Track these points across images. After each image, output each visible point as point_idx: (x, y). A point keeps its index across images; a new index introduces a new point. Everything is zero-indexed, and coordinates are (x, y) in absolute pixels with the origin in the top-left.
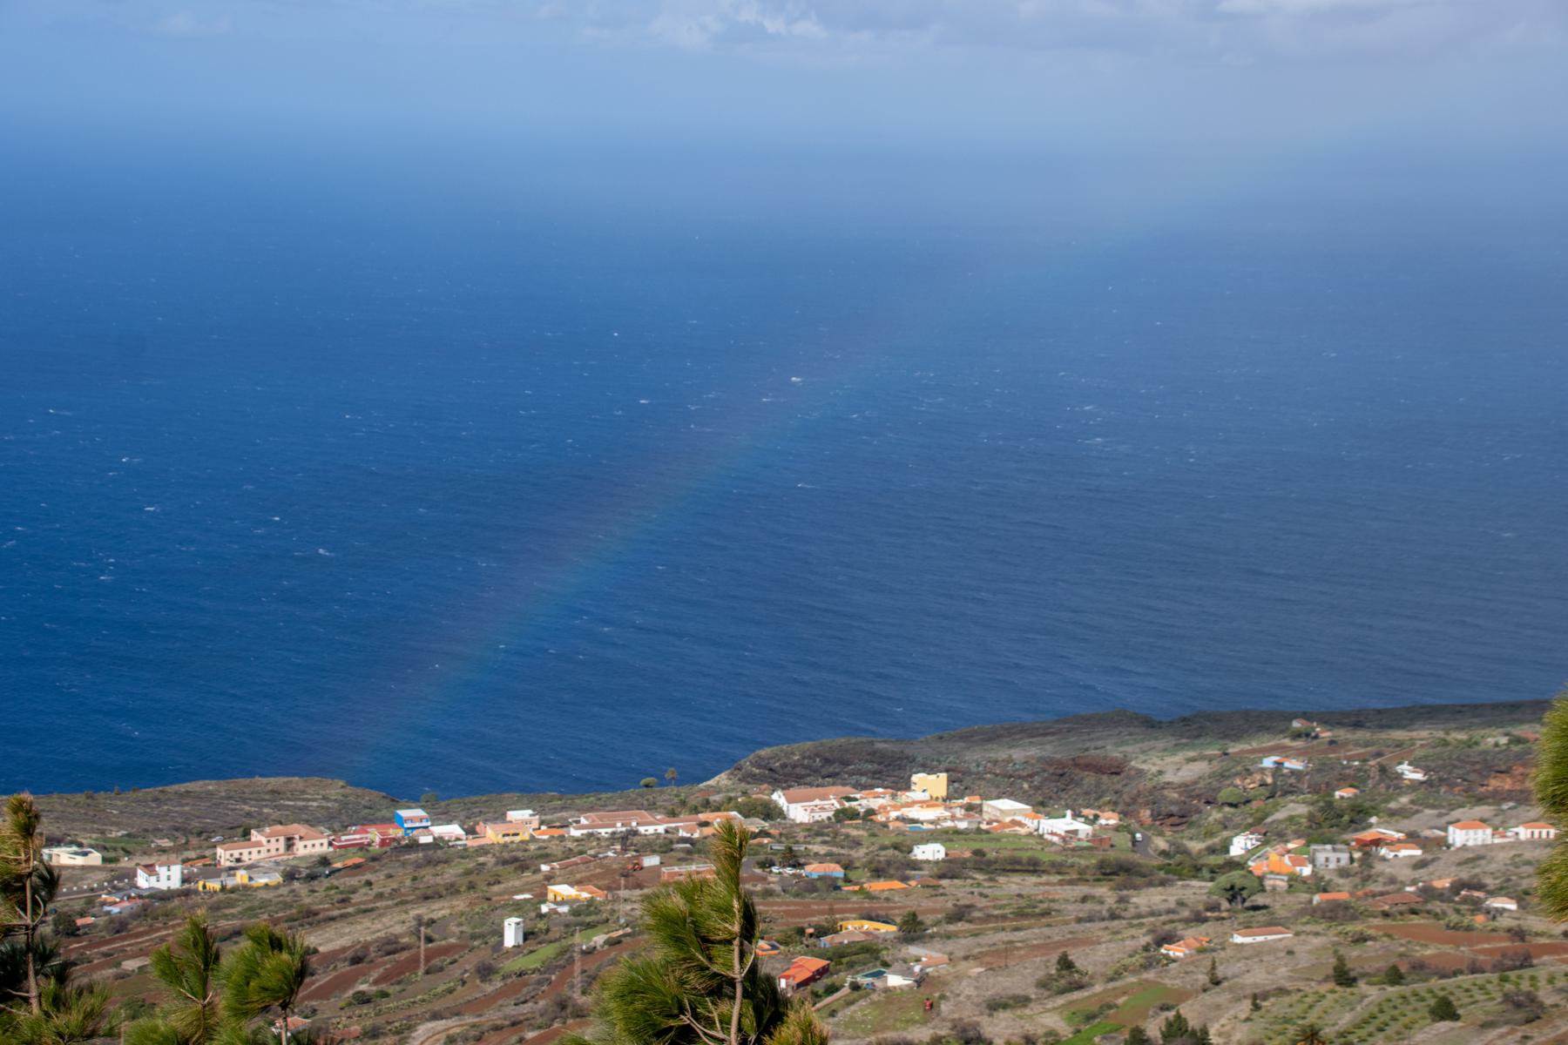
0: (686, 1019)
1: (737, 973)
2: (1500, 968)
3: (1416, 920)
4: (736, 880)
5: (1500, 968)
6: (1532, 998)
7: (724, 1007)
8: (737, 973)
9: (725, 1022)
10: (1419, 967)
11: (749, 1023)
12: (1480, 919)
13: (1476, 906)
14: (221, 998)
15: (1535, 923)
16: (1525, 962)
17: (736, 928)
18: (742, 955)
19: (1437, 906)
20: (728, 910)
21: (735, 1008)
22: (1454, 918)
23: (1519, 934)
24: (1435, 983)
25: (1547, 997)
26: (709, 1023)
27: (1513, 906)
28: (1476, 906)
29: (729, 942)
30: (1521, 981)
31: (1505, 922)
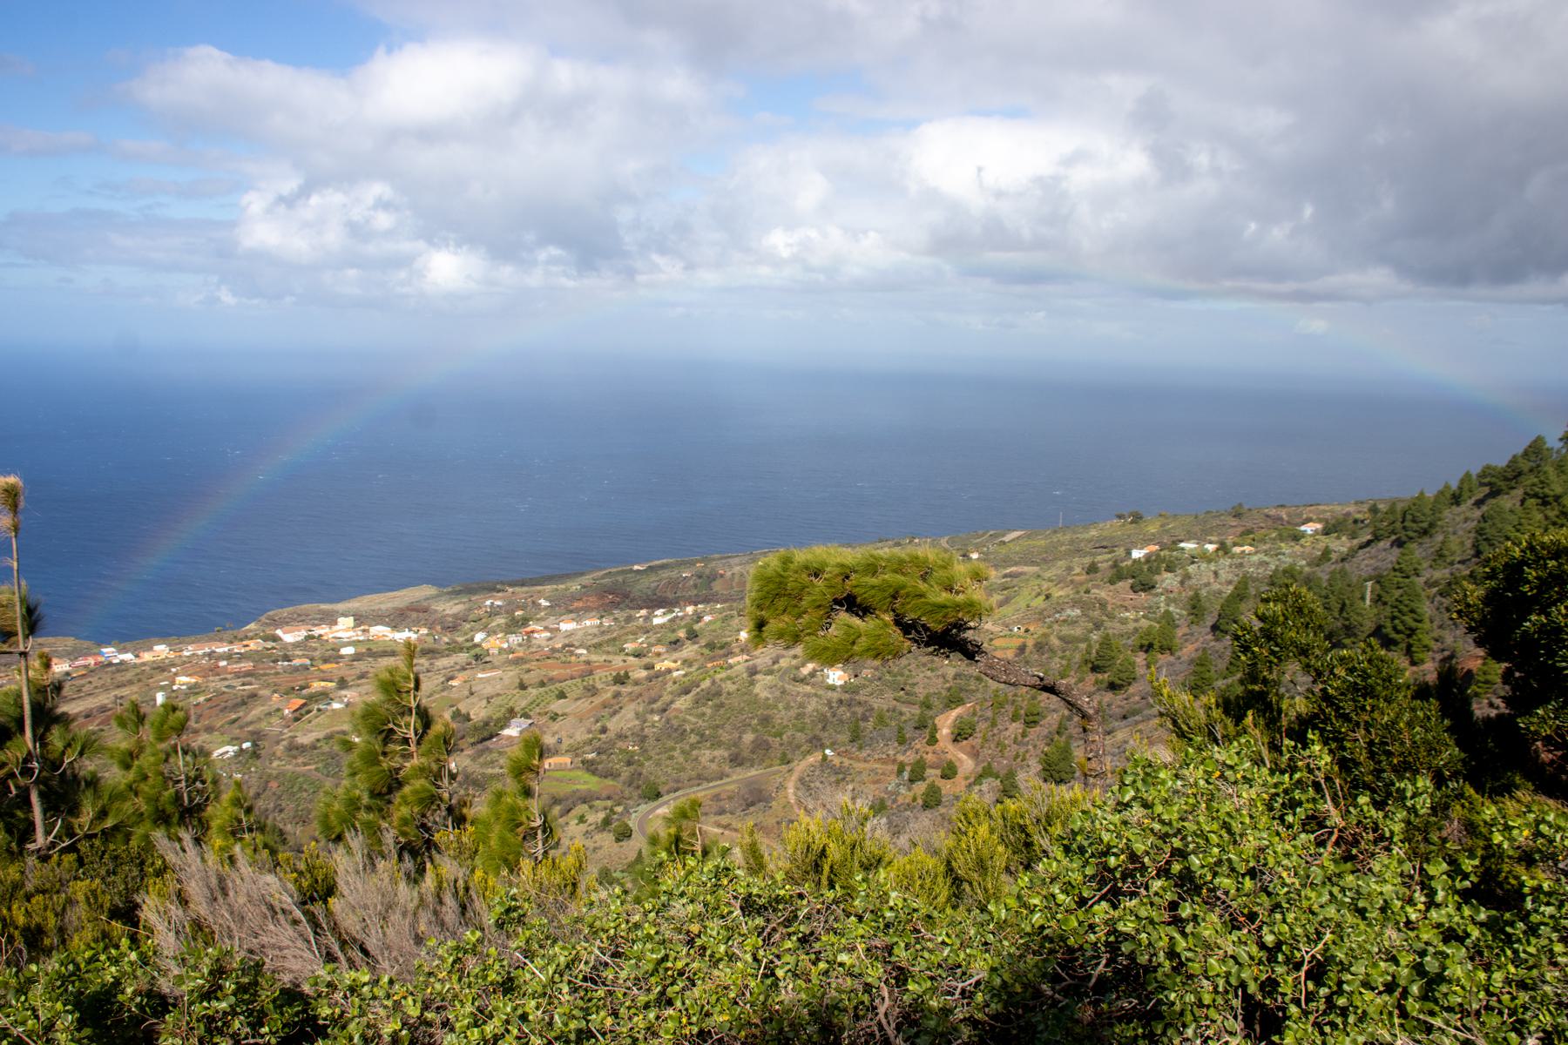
0: (391, 726)
1: (413, 705)
2: (582, 676)
3: (549, 661)
4: (411, 665)
5: (582, 676)
6: (594, 687)
7: (407, 718)
8: (413, 705)
9: (408, 725)
10: (551, 679)
11: (419, 726)
12: (573, 658)
13: (572, 653)
14: (147, 733)
15: (594, 658)
16: (591, 673)
17: (412, 685)
18: (415, 697)
19: (557, 655)
20: (409, 678)
21: (413, 719)
22: (564, 659)
23: (588, 663)
24: (558, 685)
25: (599, 686)
26: (400, 727)
27: (585, 652)
28: (572, 653)
29: (408, 692)
30: (589, 681)
31: (583, 658)
